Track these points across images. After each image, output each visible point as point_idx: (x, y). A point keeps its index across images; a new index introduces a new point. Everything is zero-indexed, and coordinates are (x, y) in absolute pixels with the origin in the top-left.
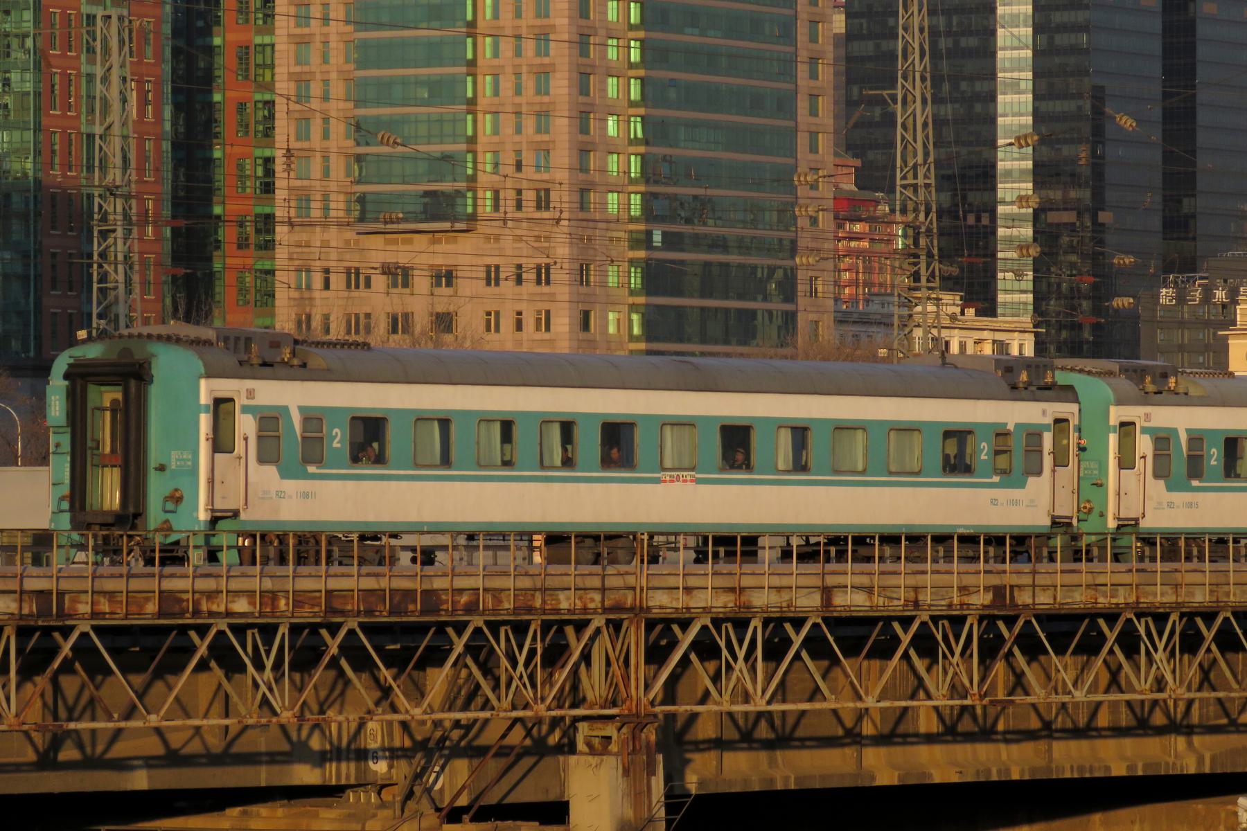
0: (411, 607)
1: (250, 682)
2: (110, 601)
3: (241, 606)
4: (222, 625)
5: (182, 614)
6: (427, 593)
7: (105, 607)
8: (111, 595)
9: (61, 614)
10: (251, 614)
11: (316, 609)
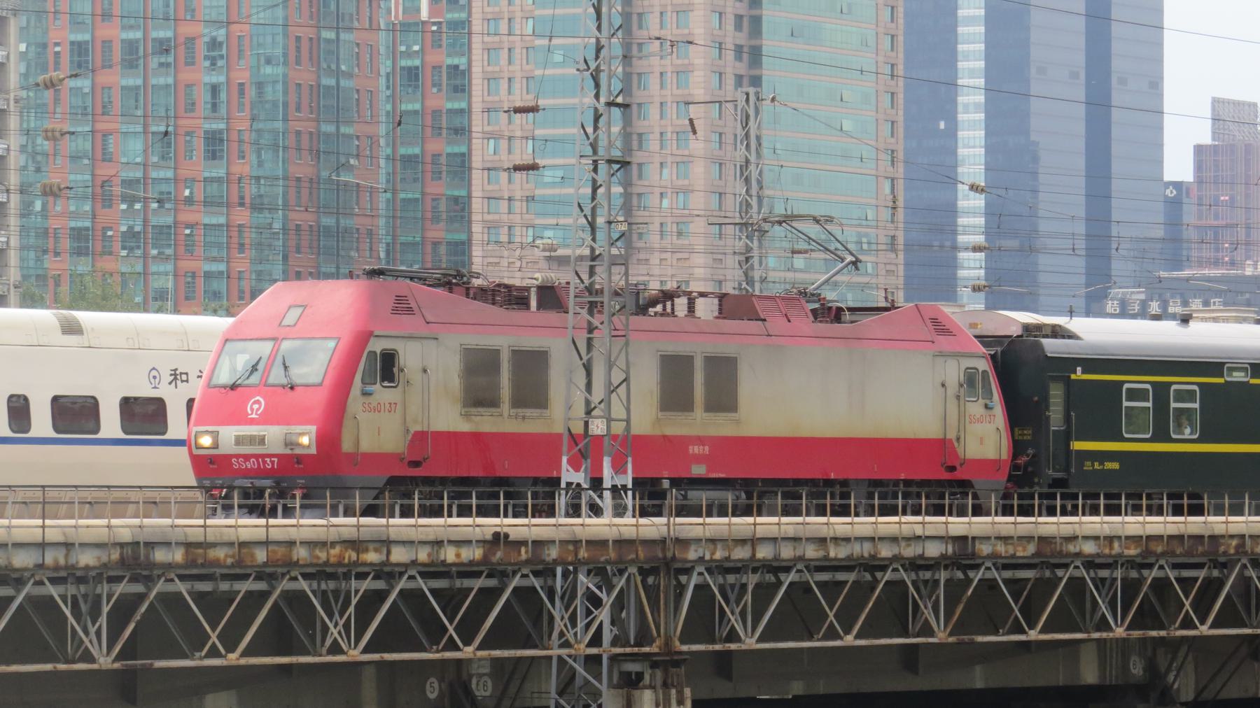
0: (1200, 549)
1: (1088, 605)
2: (1006, 544)
3: (1089, 548)
4: (1078, 563)
5: (1052, 556)
6: (1213, 538)
7: (1001, 548)
8: (1005, 539)
9: (974, 555)
10: (1098, 555)
11: (1137, 551)
